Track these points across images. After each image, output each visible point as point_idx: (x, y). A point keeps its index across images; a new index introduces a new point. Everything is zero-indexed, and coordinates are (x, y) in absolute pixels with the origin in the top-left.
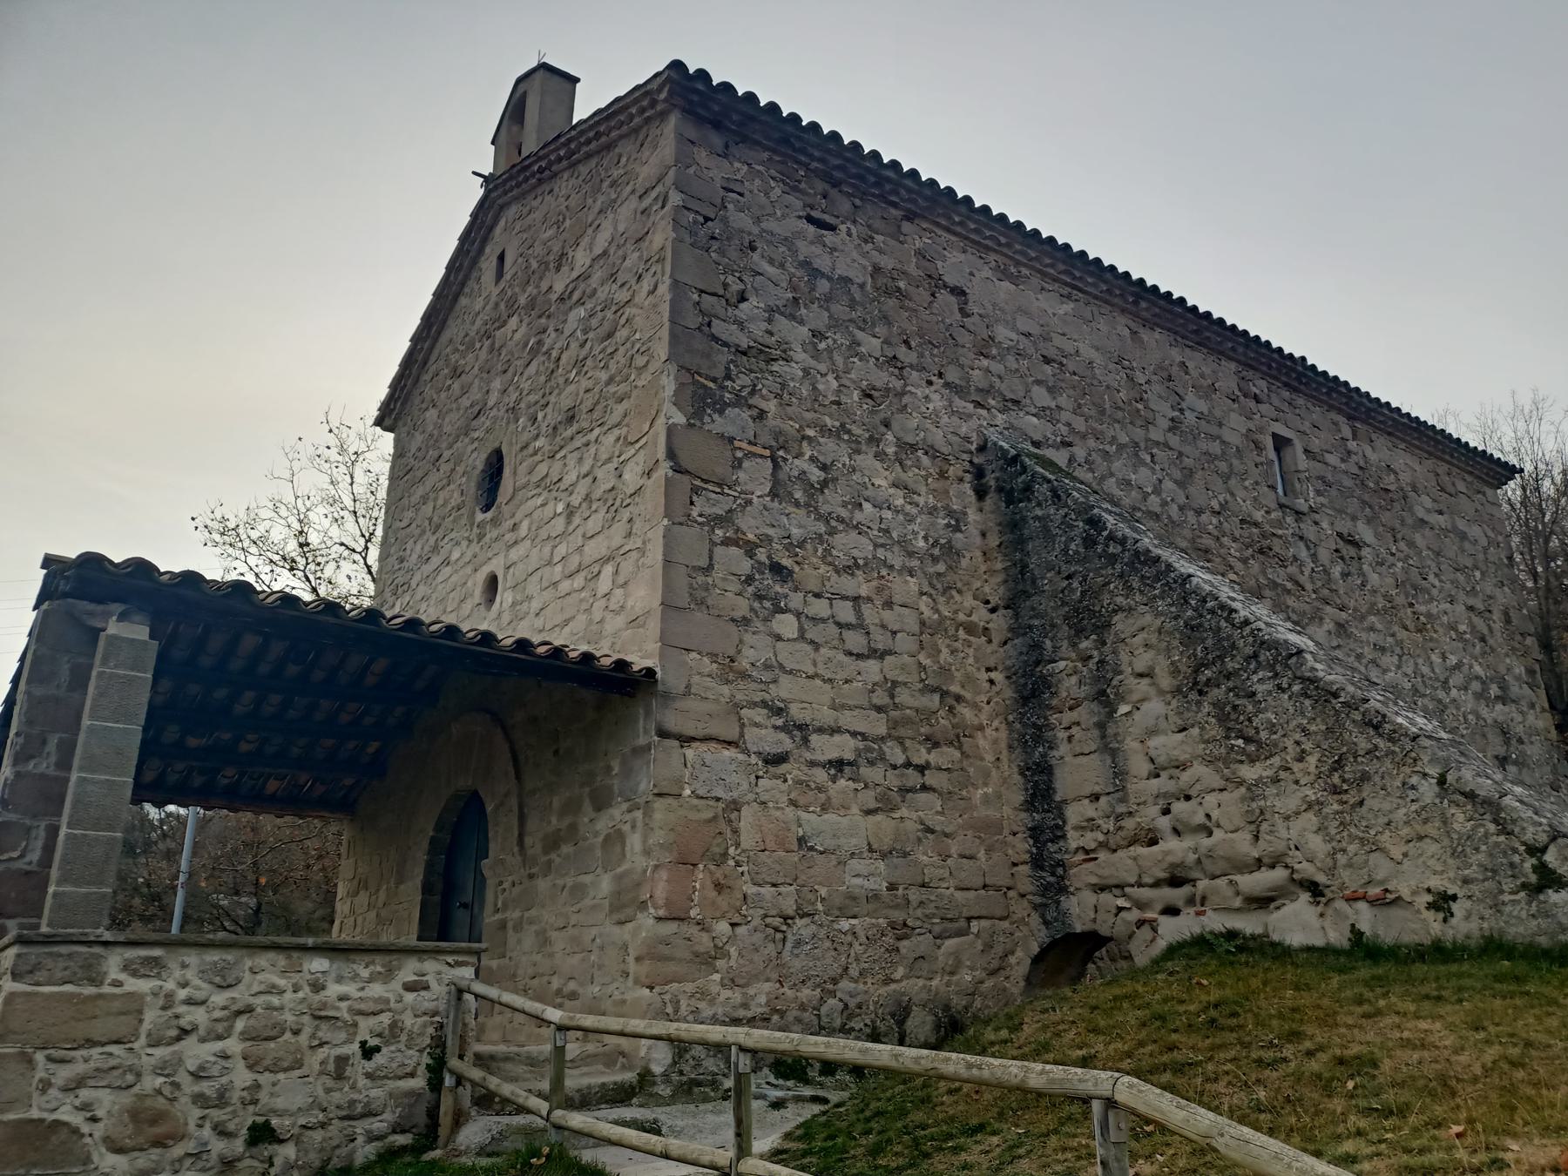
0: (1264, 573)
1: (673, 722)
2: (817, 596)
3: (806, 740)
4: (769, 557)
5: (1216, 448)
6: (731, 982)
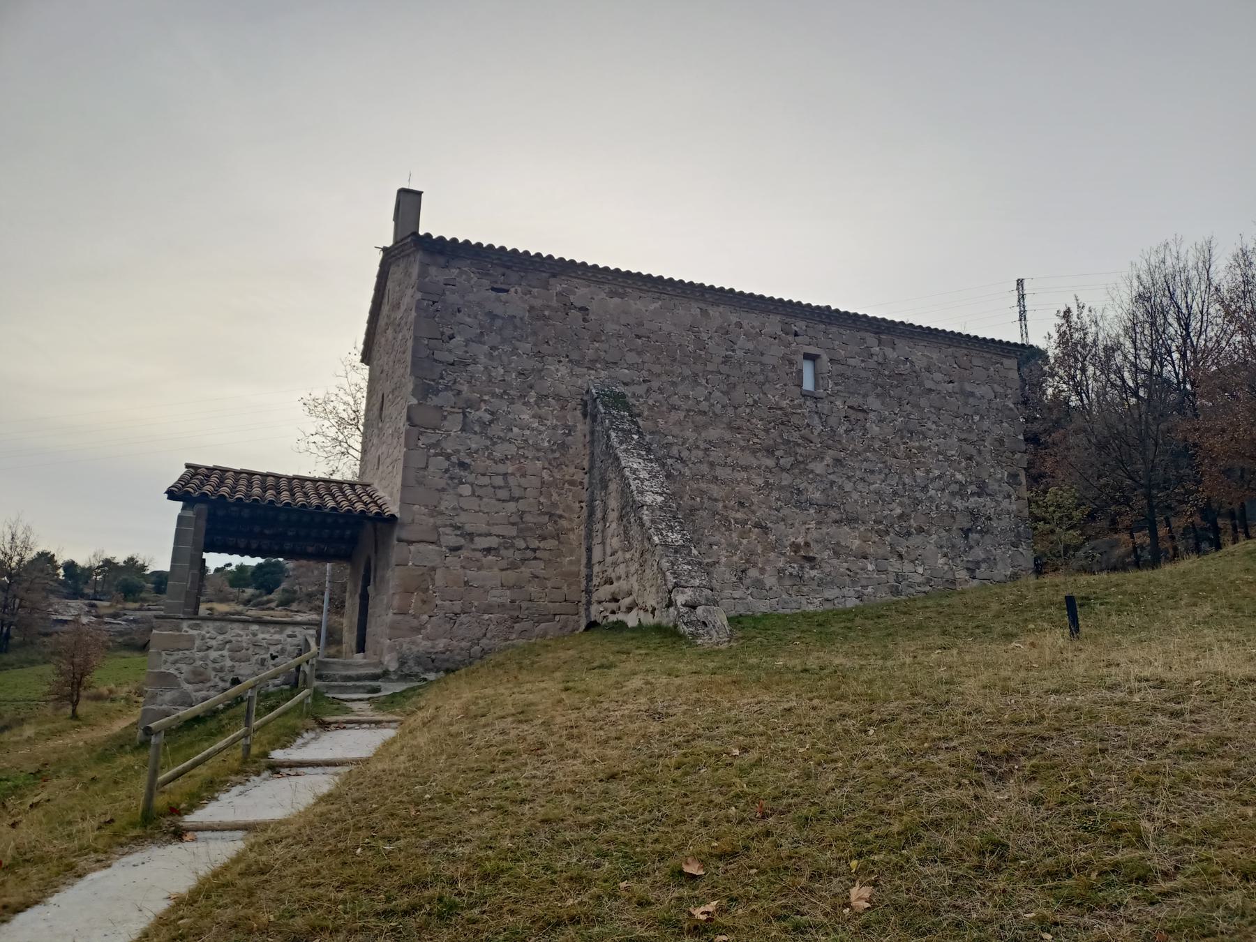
0: (781, 436)
1: (404, 534)
2: (483, 475)
3: (472, 540)
4: (458, 459)
5: (757, 368)
6: (427, 638)
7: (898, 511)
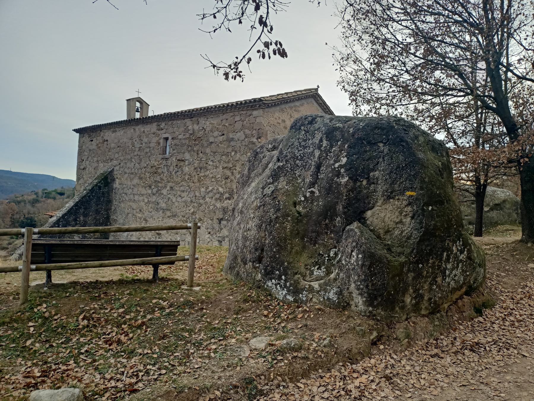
7: (192, 210)
